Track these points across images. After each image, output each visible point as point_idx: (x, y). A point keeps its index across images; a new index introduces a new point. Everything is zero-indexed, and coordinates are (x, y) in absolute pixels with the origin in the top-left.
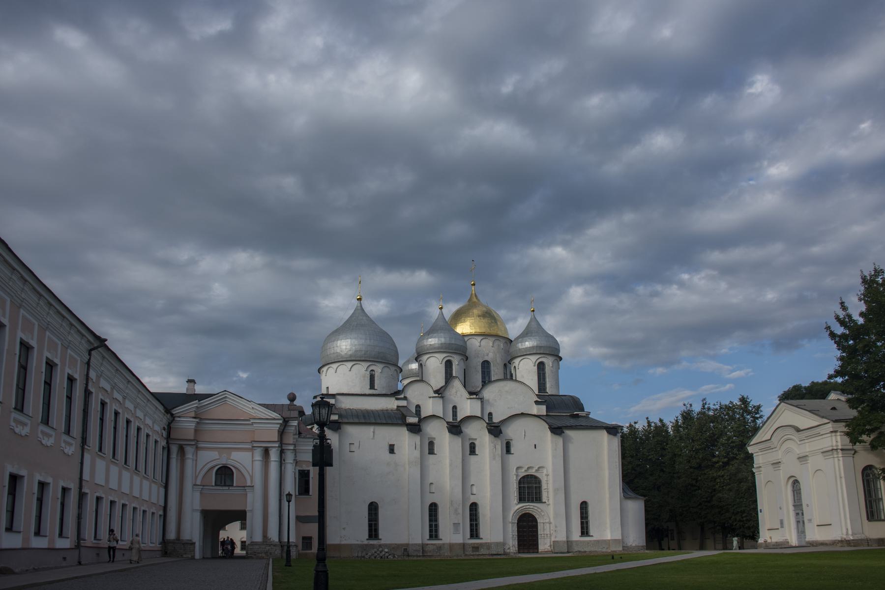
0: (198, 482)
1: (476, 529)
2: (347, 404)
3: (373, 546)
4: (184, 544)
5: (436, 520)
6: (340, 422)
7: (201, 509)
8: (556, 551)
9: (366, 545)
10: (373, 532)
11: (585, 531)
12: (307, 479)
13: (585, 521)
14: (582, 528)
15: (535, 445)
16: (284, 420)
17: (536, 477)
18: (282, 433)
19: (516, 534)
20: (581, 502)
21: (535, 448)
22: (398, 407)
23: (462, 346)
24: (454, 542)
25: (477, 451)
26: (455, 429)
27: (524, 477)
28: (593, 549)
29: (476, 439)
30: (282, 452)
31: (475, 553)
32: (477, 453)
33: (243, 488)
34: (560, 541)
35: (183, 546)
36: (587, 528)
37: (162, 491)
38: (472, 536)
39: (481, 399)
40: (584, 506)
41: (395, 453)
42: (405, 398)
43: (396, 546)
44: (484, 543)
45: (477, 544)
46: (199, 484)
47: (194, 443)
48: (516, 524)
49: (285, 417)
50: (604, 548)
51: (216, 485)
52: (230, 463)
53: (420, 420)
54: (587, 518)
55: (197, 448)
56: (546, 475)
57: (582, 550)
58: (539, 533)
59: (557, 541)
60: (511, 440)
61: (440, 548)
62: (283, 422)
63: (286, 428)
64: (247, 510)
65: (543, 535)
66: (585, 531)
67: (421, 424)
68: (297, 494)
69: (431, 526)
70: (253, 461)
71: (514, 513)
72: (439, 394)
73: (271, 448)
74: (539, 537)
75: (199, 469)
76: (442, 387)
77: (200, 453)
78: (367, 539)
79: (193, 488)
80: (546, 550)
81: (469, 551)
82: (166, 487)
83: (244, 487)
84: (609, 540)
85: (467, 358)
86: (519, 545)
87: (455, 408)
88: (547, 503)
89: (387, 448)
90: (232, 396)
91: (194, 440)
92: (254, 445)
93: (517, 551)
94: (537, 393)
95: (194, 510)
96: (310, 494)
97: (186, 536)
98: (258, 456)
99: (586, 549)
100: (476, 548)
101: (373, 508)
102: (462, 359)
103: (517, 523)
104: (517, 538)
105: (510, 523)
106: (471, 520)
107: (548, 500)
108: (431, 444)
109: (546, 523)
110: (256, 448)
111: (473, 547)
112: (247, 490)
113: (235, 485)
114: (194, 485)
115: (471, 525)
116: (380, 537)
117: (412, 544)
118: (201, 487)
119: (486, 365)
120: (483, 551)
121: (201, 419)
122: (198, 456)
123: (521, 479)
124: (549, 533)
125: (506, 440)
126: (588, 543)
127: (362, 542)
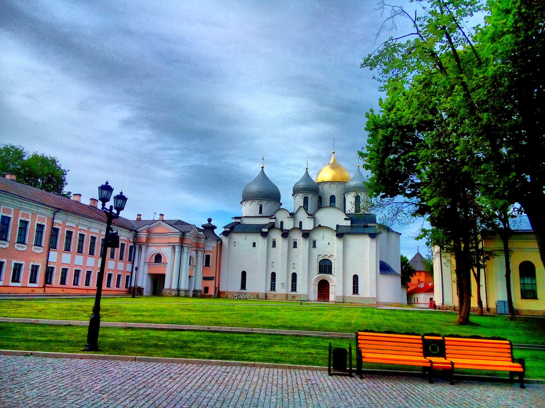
2: (246, 221)
3: (242, 293)
5: (275, 281)
9: (239, 293)
11: (356, 290)
26: (285, 234)
30: (182, 247)
37: (129, 266)
38: (292, 290)
40: (356, 278)
42: (275, 218)
51: (155, 262)
52: (161, 252)
54: (357, 284)
61: (275, 296)
66: (356, 290)
68: (204, 265)
69: (272, 284)
79: (144, 264)
86: (318, 297)
89: (252, 244)
97: (139, 285)
101: (244, 274)
119: (333, 198)
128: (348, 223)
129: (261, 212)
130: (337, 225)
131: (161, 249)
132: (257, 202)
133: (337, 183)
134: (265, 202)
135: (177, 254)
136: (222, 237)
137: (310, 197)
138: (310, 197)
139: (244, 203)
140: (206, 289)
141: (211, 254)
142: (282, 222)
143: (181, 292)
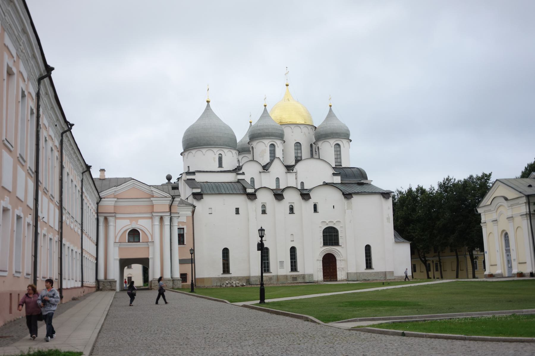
0: (117, 241)
1: (295, 265)
4: (110, 282)
6: (202, 194)
7: (119, 258)
8: (349, 280)
9: (221, 278)
10: (226, 269)
11: (369, 265)
12: (182, 233)
13: (368, 258)
14: (367, 263)
15: (334, 206)
16: (172, 197)
17: (334, 228)
18: (170, 207)
19: (322, 268)
20: (366, 245)
21: (334, 208)
22: (238, 180)
23: (281, 133)
24: (279, 274)
25: (295, 210)
26: (279, 195)
27: (326, 228)
28: (374, 278)
29: (294, 203)
31: (294, 282)
32: (294, 213)
33: (146, 243)
34: (352, 273)
35: (109, 283)
36: (370, 263)
39: (295, 172)
40: (368, 248)
41: (239, 214)
43: (241, 278)
44: (300, 275)
45: (296, 275)
46: (118, 242)
47: (114, 215)
48: (322, 261)
49: (172, 195)
50: (382, 277)
51: (129, 242)
53: (255, 191)
55: (116, 218)
56: (341, 227)
57: (367, 279)
58: (337, 267)
59: (350, 273)
60: (317, 203)
62: (172, 199)
63: (173, 202)
64: (149, 257)
65: (340, 269)
66: (369, 265)
67: (256, 193)
70: (152, 225)
71: (320, 253)
72: (267, 170)
73: (165, 217)
74: (337, 270)
75: (117, 232)
76: (268, 164)
77: (118, 221)
78: (222, 274)
79: (114, 244)
80: (342, 279)
81: (290, 281)
82: (97, 245)
83: (147, 242)
84: (385, 272)
85: (284, 142)
87: (278, 179)
88: (342, 246)
90: (137, 183)
91: (114, 213)
92: (154, 215)
93: (323, 280)
94: (334, 166)
95: (115, 259)
96: (185, 244)
98: (157, 222)
99: (369, 278)
100: (295, 278)
101: (226, 252)
102: (282, 143)
103: (322, 260)
104: (322, 271)
105: (317, 260)
106: (291, 259)
107: (343, 244)
108: (264, 206)
109: (343, 260)
110: (155, 217)
111: (293, 278)
112: (149, 245)
113: (141, 241)
114: (115, 242)
115: (291, 262)
116: (230, 273)
117: (252, 277)
118: (119, 244)
119: (298, 145)
120: (300, 280)
121: (118, 198)
122: (116, 224)
123: (324, 230)
124: (344, 267)
125: (314, 203)
126: (371, 274)
127: (219, 276)
128: (337, 180)
129: (220, 165)
130: (324, 182)
131: (137, 222)
132: (215, 150)
133: (302, 127)
134: (226, 151)
135: (167, 228)
136: (191, 200)
137: (278, 144)
138: (278, 144)
139: (194, 152)
140: (184, 277)
141: (185, 227)
142: (252, 180)
143: (176, 282)
